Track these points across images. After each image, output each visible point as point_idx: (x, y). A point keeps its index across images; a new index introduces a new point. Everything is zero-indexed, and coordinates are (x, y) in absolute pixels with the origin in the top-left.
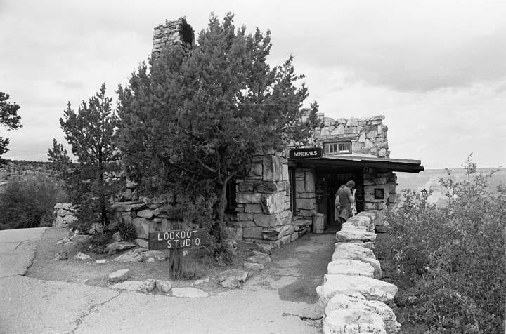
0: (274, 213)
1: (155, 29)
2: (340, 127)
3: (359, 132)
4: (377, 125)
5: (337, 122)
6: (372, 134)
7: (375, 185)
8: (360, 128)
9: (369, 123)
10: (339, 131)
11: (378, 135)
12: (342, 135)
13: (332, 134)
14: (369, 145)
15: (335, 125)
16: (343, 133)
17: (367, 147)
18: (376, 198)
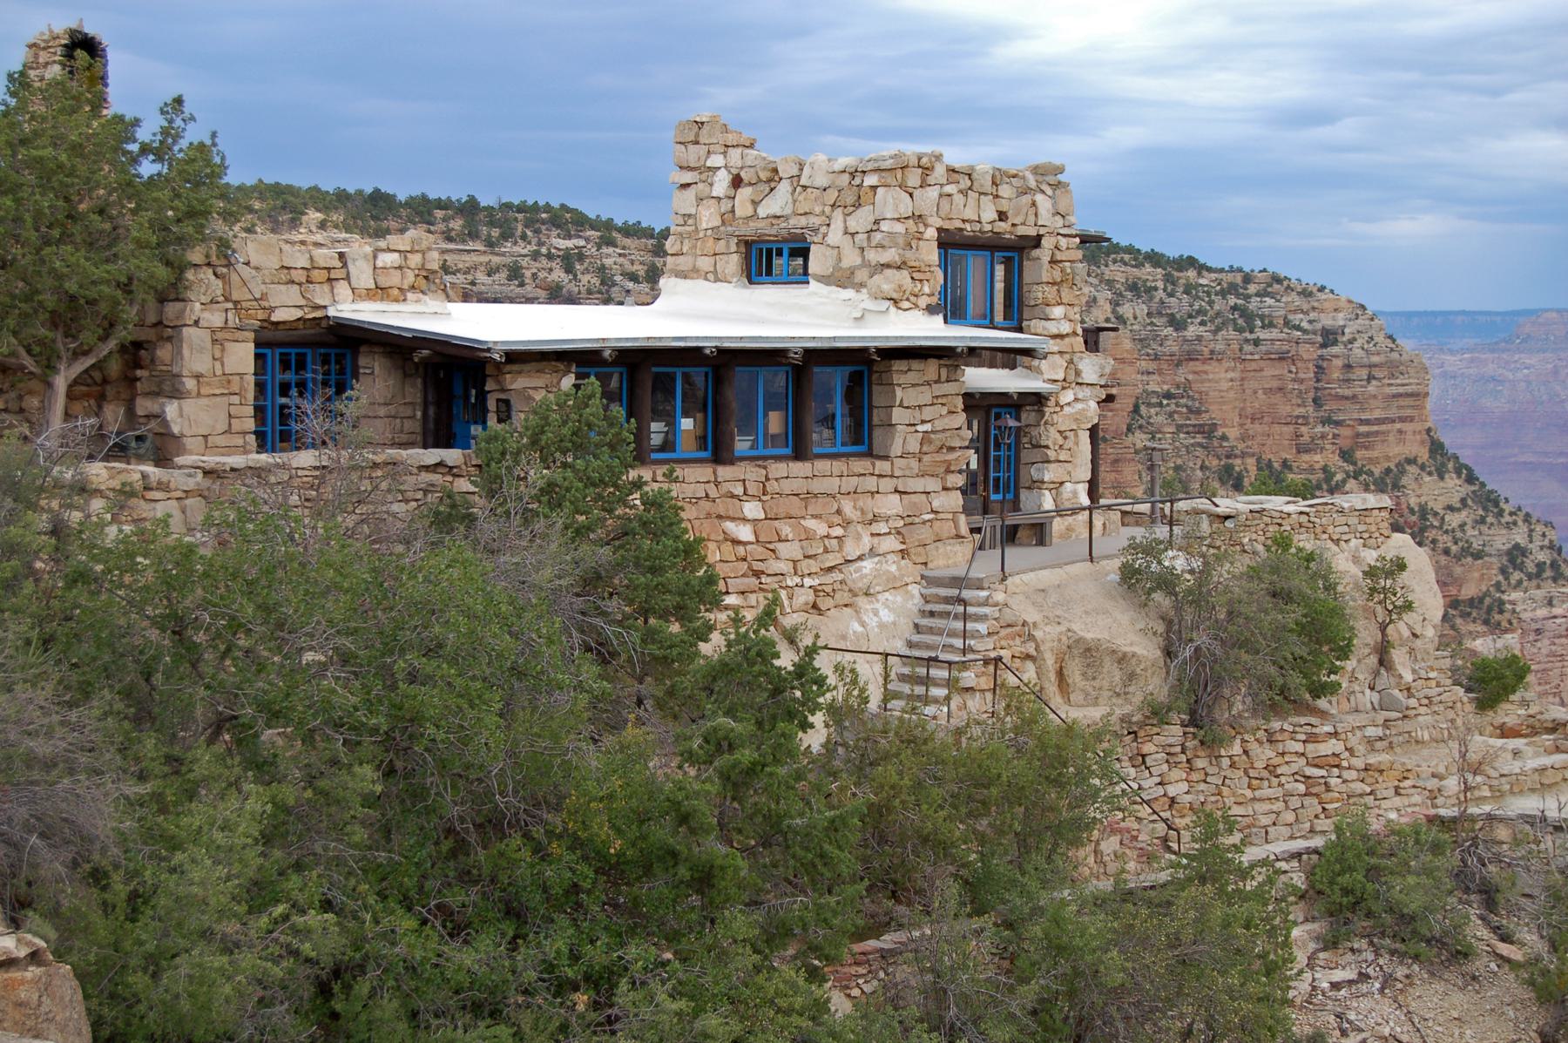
0: (183, 435)
1: (30, 46)
2: (784, 188)
3: (828, 209)
4: (874, 188)
5: (775, 171)
6: (861, 220)
7: (503, 390)
8: (831, 196)
9: (857, 181)
10: (778, 202)
11: (877, 222)
12: (787, 218)
13: (762, 212)
14: (851, 258)
15: (770, 180)
16: (788, 211)
17: (845, 264)
18: (500, 421)
